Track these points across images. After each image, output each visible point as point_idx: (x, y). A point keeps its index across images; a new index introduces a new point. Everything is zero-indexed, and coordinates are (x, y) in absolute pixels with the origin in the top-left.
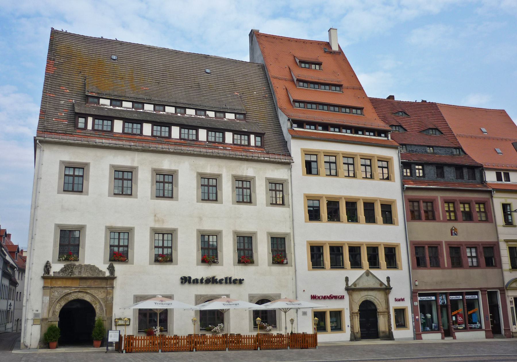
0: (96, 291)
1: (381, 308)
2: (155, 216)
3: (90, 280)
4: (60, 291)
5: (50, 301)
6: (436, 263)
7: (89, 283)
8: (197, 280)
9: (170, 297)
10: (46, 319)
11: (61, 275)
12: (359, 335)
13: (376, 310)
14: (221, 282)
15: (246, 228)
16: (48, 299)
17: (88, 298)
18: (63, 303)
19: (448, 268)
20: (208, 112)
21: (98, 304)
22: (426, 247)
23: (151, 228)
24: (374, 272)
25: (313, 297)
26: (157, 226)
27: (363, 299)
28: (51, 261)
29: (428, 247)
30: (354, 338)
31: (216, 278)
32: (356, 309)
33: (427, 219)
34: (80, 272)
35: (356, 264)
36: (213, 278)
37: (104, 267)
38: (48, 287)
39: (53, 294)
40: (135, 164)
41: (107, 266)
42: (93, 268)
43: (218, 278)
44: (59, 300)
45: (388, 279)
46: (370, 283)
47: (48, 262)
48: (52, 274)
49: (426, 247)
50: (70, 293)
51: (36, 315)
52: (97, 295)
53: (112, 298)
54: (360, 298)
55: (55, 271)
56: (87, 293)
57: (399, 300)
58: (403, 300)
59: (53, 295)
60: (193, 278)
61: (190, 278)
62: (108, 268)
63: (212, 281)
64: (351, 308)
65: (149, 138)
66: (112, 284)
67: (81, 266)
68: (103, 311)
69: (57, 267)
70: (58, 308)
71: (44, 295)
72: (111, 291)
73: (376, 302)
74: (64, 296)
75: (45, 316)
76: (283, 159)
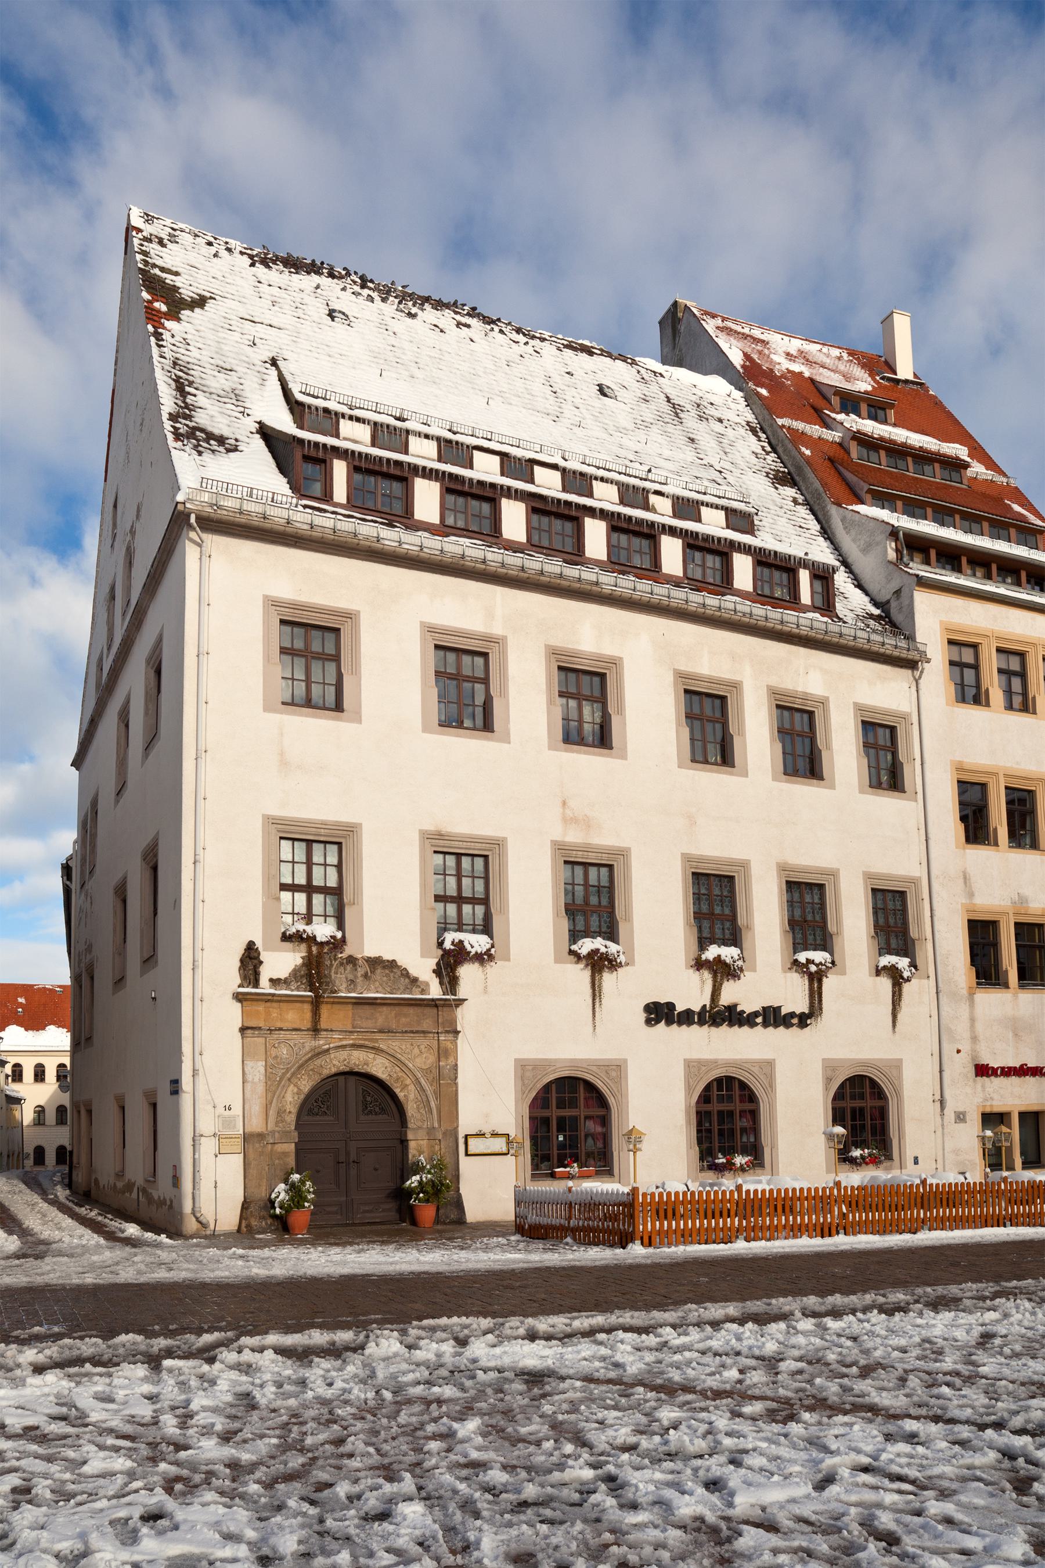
2: (564, 803)
3: (385, 1009)
4: (295, 1045)
5: (268, 1077)
7: (383, 1017)
10: (261, 1136)
16: (262, 1070)
17: (379, 1068)
18: (306, 1085)
21: (412, 1087)
23: (554, 843)
25: (982, 1070)
26: (574, 837)
28: (259, 944)
31: (739, 1009)
34: (352, 981)
38: (260, 1028)
39: (273, 1052)
44: (293, 1074)
47: (251, 947)
50: (328, 1050)
52: (409, 1059)
53: (455, 1067)
55: (275, 978)
56: (377, 1050)
59: (276, 1057)
62: (434, 971)
66: (454, 1022)
67: (352, 960)
68: (431, 1111)
70: (291, 1098)
72: (449, 1045)
74: (310, 1059)
76: (890, 643)
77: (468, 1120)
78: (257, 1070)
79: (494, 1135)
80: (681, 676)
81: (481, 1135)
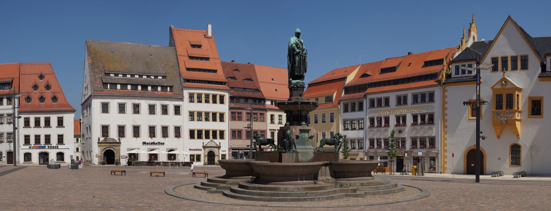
0: (115, 147)
1: (216, 154)
2: (133, 120)
6: (240, 137)
8: (148, 143)
9: (139, 149)
11: (103, 142)
12: (207, 163)
13: (215, 154)
14: (156, 143)
15: (165, 124)
17: (112, 149)
18: (104, 151)
19: (244, 140)
20: (151, 77)
22: (237, 131)
24: (214, 140)
25: (190, 150)
27: (209, 150)
29: (238, 131)
30: (205, 164)
32: (206, 154)
33: (239, 120)
35: (207, 137)
36: (154, 142)
37: (117, 139)
40: (126, 102)
41: (118, 138)
42: (113, 139)
43: (155, 142)
45: (220, 143)
46: (212, 144)
47: (99, 137)
48: (100, 141)
49: (237, 131)
51: (97, 155)
54: (207, 150)
57: (224, 151)
58: (225, 151)
60: (147, 142)
61: (146, 142)
63: (153, 143)
64: (204, 154)
65: (130, 91)
69: (102, 139)
70: (103, 152)
71: (99, 148)
73: (214, 151)
75: (99, 155)
77: (121, 154)
78: (100, 149)
79: (124, 156)
80: (149, 104)
81: (123, 156)
